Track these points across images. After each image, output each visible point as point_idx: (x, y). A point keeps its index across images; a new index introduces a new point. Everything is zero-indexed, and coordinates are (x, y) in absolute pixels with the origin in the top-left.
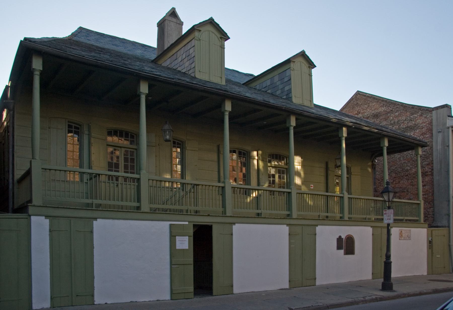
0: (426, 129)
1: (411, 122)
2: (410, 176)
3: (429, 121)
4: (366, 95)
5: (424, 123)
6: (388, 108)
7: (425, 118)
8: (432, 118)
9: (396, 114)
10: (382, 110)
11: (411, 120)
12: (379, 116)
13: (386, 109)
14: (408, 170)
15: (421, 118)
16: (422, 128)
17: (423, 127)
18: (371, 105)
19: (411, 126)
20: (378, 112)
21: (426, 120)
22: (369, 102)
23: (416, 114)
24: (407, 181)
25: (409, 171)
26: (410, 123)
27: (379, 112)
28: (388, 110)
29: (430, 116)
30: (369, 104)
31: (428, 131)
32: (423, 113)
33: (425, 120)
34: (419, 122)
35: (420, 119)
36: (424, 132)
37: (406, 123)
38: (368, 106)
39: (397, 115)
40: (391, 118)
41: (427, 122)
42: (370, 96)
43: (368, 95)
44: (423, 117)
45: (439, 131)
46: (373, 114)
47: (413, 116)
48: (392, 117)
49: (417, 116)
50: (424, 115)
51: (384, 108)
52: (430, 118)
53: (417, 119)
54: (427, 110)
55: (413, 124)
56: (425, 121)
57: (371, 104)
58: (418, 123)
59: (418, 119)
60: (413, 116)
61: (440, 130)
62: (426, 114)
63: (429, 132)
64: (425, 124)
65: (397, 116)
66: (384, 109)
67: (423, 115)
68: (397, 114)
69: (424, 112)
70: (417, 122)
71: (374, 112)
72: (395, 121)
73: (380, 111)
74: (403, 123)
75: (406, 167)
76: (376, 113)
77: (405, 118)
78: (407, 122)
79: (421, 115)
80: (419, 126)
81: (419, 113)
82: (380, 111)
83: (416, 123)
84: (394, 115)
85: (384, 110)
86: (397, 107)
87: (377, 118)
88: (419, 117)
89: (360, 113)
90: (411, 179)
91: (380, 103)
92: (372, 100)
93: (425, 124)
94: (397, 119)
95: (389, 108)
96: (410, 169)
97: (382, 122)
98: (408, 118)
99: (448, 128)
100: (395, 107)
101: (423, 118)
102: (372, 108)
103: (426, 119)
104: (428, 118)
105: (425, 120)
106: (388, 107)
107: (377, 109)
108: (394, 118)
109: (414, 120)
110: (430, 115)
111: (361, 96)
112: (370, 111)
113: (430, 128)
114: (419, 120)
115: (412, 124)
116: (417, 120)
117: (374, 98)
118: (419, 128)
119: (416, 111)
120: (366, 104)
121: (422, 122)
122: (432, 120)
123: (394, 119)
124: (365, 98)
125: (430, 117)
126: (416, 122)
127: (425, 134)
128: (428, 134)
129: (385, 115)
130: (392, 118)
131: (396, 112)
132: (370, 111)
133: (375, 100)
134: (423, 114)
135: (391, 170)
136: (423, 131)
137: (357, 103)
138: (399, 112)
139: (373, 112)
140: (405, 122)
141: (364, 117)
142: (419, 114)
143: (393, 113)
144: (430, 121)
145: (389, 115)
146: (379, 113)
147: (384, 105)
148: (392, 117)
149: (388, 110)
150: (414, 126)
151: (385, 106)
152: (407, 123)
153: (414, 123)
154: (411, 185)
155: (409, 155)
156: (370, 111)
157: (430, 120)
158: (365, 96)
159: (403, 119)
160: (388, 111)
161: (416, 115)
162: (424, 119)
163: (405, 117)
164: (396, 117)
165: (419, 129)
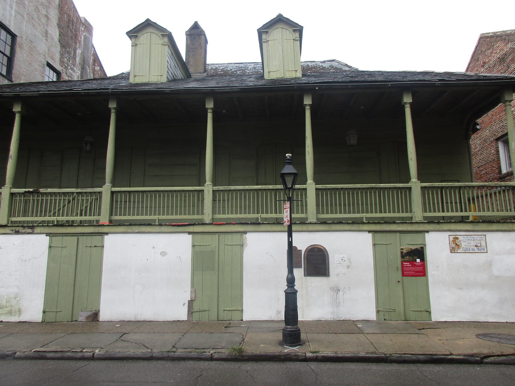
12: (506, 59)
20: (503, 54)
27: (505, 52)
46: (499, 58)
76: (502, 55)
87: (504, 63)
89: (485, 63)
97: (510, 66)
111: (485, 39)
112: (496, 56)
117: (498, 36)
120: (490, 49)
124: (488, 39)
132: (496, 56)
137: (481, 51)
141: (490, 67)
156: (495, 56)
158: (487, 37)
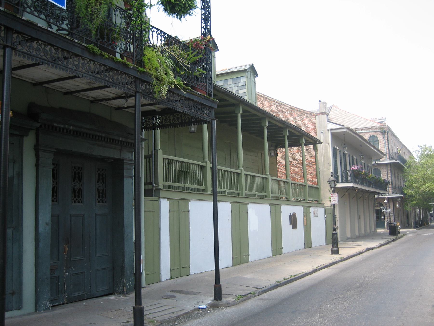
0: (311, 128)
1: (298, 122)
2: (299, 164)
3: (312, 123)
4: (259, 94)
5: (309, 124)
6: (278, 108)
7: (310, 120)
8: (315, 120)
9: (286, 113)
10: (274, 109)
11: (299, 120)
13: (277, 109)
14: (298, 160)
15: (306, 119)
16: (308, 127)
17: (309, 127)
18: (263, 103)
19: (298, 124)
20: (270, 110)
21: (311, 122)
22: (261, 100)
23: (302, 116)
24: (297, 169)
25: (298, 160)
26: (298, 122)
28: (279, 109)
29: (313, 119)
30: (261, 102)
31: (312, 130)
32: (308, 116)
33: (310, 122)
34: (305, 122)
35: (305, 120)
36: (309, 131)
37: (294, 122)
38: (261, 104)
39: (286, 114)
40: (281, 116)
41: (312, 123)
42: (263, 95)
43: (260, 94)
44: (308, 119)
45: (321, 131)
47: (300, 117)
48: (283, 116)
49: (303, 117)
50: (309, 117)
51: (275, 107)
52: (314, 121)
53: (303, 120)
54: (311, 114)
55: (300, 123)
56: (309, 122)
57: (263, 102)
58: (304, 123)
59: (304, 120)
60: (300, 117)
61: (322, 131)
62: (310, 117)
63: (313, 131)
64: (310, 125)
65: (287, 115)
66: (275, 108)
67: (307, 118)
68: (286, 113)
69: (308, 115)
70: (303, 122)
71: (266, 109)
72: (285, 119)
73: (272, 109)
74: (292, 121)
75: (295, 157)
77: (293, 118)
78: (295, 122)
79: (306, 117)
80: (305, 126)
81: (305, 116)
82: (272, 109)
83: (303, 123)
84: (284, 114)
85: (275, 109)
86: (286, 108)
88: (304, 119)
90: (300, 167)
91: (272, 103)
92: (265, 99)
93: (310, 125)
94: (287, 117)
95: (280, 108)
96: (299, 159)
98: (295, 118)
99: (328, 130)
100: (285, 108)
101: (308, 119)
102: (265, 106)
103: (311, 121)
104: (312, 120)
105: (310, 122)
106: (278, 107)
107: (269, 107)
108: (284, 116)
109: (301, 120)
110: (313, 118)
113: (314, 128)
114: (305, 121)
115: (299, 124)
116: (303, 120)
118: (305, 127)
119: (302, 114)
121: (307, 123)
122: (316, 122)
123: (284, 117)
125: (314, 120)
126: (302, 122)
127: (310, 132)
128: (312, 132)
129: (276, 113)
130: (282, 116)
131: (286, 112)
133: (267, 100)
134: (308, 117)
135: (283, 159)
136: (309, 130)
138: (288, 112)
139: (266, 109)
140: (293, 121)
142: (304, 116)
143: (283, 113)
144: (313, 123)
145: (280, 113)
146: (271, 111)
147: (275, 104)
148: (282, 115)
149: (279, 109)
150: (300, 125)
151: (276, 106)
152: (295, 122)
153: (301, 123)
154: (300, 172)
155: (295, 148)
157: (314, 122)
159: (291, 118)
160: (278, 110)
161: (302, 117)
162: (309, 121)
163: (293, 117)
164: (286, 116)
165: (306, 128)
